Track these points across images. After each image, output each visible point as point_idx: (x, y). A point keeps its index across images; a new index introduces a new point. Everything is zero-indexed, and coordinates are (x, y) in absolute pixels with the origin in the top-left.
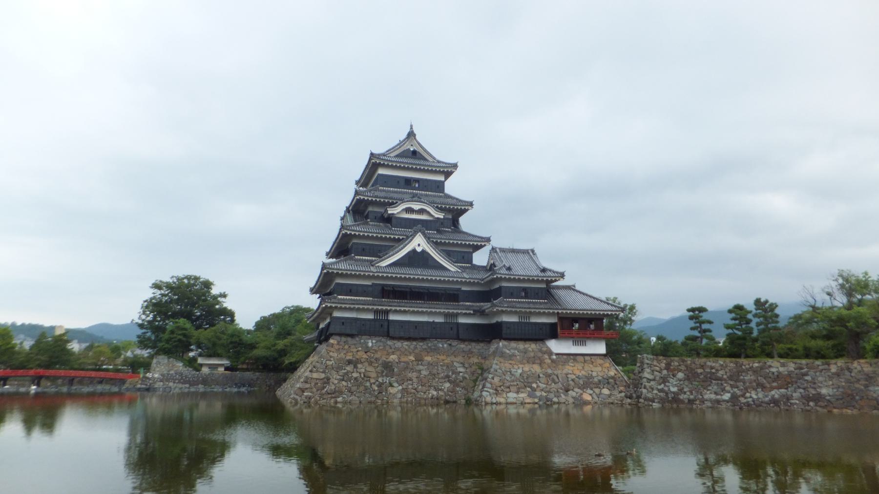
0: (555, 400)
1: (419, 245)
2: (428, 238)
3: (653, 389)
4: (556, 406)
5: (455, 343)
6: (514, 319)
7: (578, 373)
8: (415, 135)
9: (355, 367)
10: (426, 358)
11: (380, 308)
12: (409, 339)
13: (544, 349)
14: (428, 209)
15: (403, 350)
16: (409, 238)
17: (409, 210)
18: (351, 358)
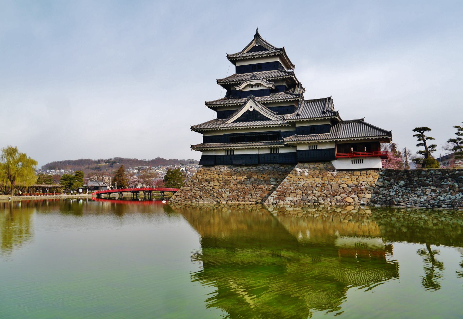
0: (322, 202)
1: (251, 107)
3: (380, 194)
4: (322, 206)
5: (276, 166)
6: (306, 148)
7: (350, 183)
9: (209, 183)
10: (254, 177)
12: (246, 165)
13: (329, 167)
14: (261, 83)
15: (242, 172)
16: (245, 103)
17: (250, 86)
18: (208, 178)
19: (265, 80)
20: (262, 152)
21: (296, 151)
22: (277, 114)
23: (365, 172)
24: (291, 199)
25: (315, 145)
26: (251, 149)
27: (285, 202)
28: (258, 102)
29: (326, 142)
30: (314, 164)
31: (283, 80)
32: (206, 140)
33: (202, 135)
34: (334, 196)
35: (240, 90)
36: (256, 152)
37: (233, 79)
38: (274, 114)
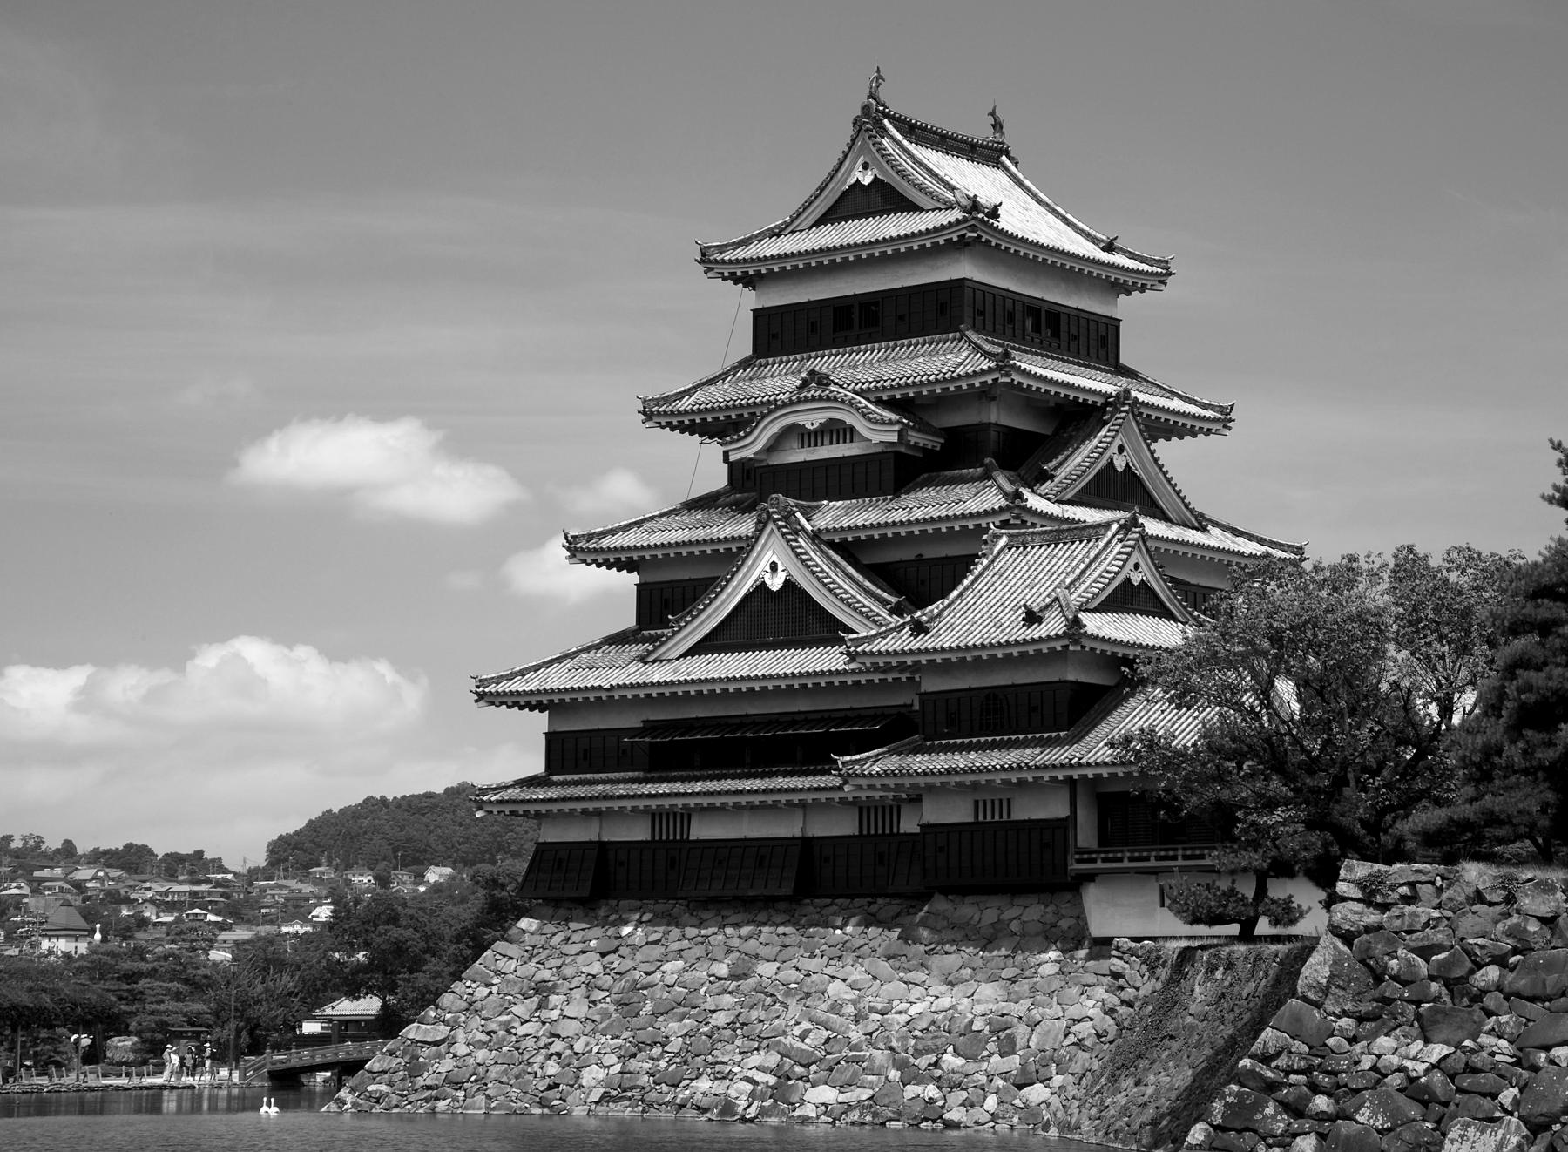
0: (954, 1115)
1: (774, 567)
13: (1064, 924)
14: (850, 419)
18: (545, 974)
21: (918, 830)
24: (827, 1094)
25: (1004, 797)
26: (751, 807)
27: (797, 1113)
28: (815, 537)
29: (1021, 783)
32: (565, 753)
33: (540, 722)
34: (1020, 1087)
36: (787, 828)
37: (717, 395)
38: (884, 603)
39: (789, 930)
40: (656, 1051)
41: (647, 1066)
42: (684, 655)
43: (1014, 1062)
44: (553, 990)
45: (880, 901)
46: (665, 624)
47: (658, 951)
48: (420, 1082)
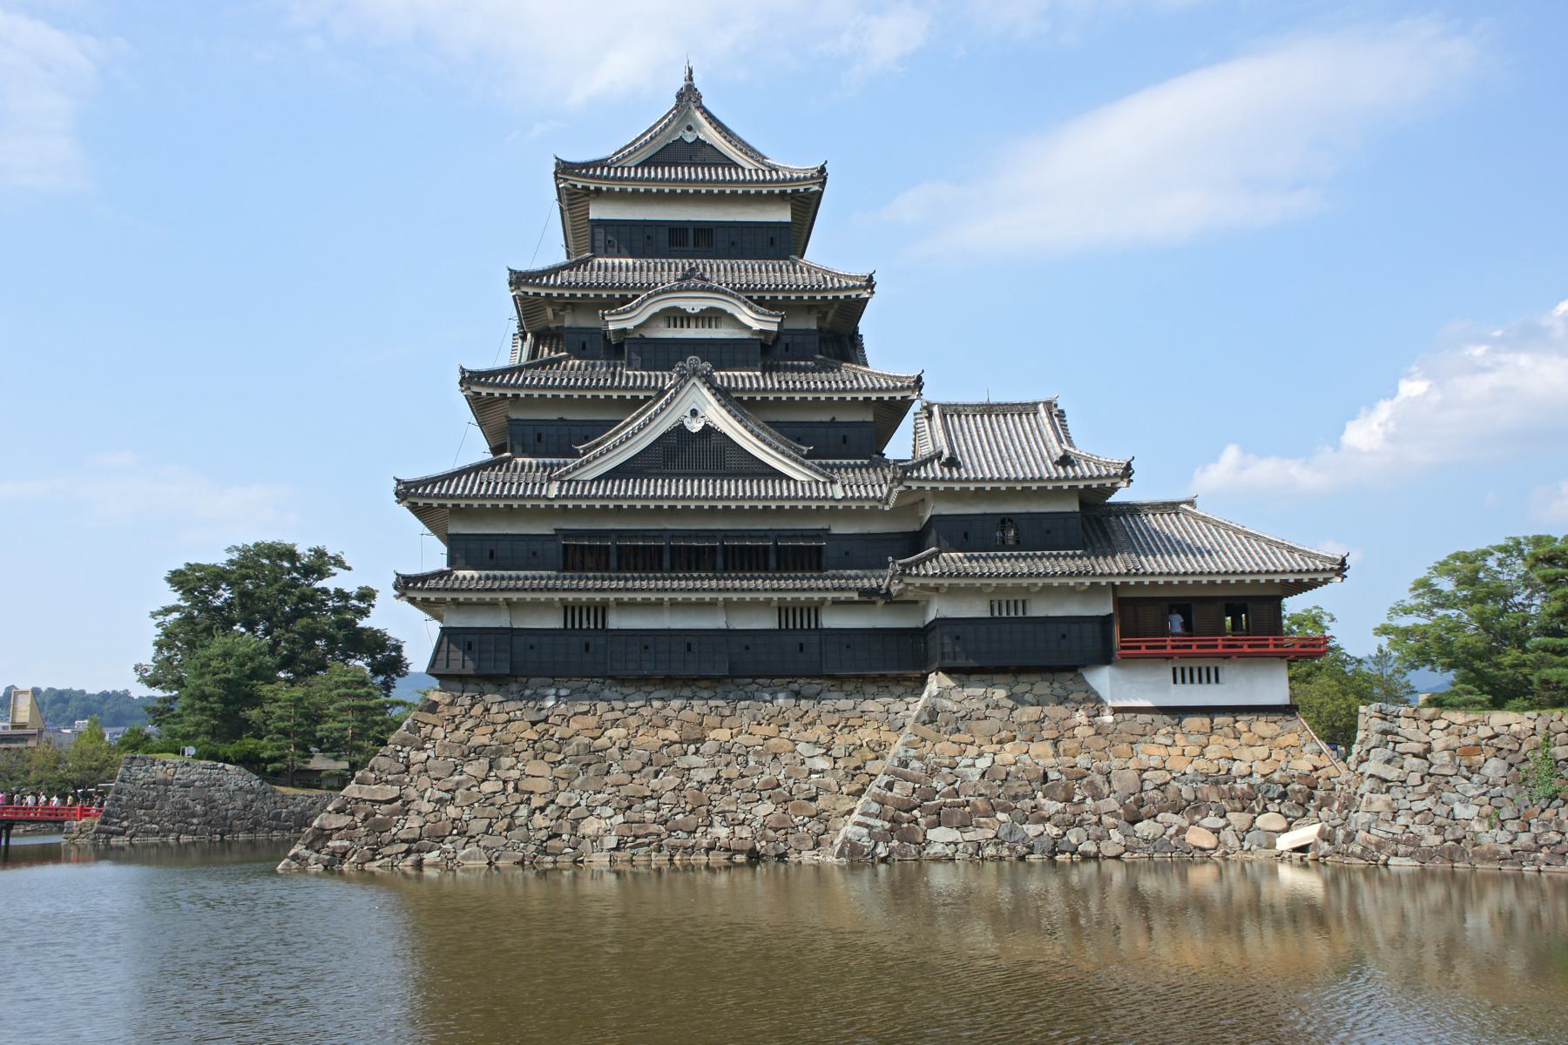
0: (1090, 847)
1: (694, 413)
2: (724, 395)
8: (699, 97)
11: (584, 597)
14: (729, 309)
18: (485, 740)
19: (742, 297)
20: (742, 622)
22: (807, 457)
23: (1228, 719)
25: (1020, 598)
30: (1009, 678)
31: (810, 307)
32: (461, 550)
34: (1133, 823)
35: (624, 330)
38: (798, 451)
39: (721, 703)
40: (650, 803)
41: (650, 816)
42: (599, 479)
43: (1112, 803)
44: (499, 753)
45: (801, 681)
46: (576, 455)
47: (591, 721)
48: (386, 836)
